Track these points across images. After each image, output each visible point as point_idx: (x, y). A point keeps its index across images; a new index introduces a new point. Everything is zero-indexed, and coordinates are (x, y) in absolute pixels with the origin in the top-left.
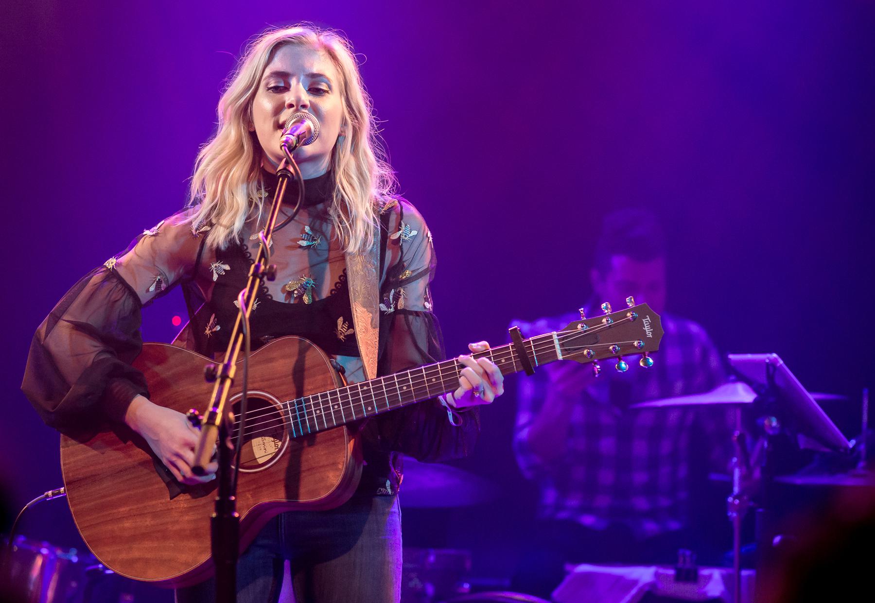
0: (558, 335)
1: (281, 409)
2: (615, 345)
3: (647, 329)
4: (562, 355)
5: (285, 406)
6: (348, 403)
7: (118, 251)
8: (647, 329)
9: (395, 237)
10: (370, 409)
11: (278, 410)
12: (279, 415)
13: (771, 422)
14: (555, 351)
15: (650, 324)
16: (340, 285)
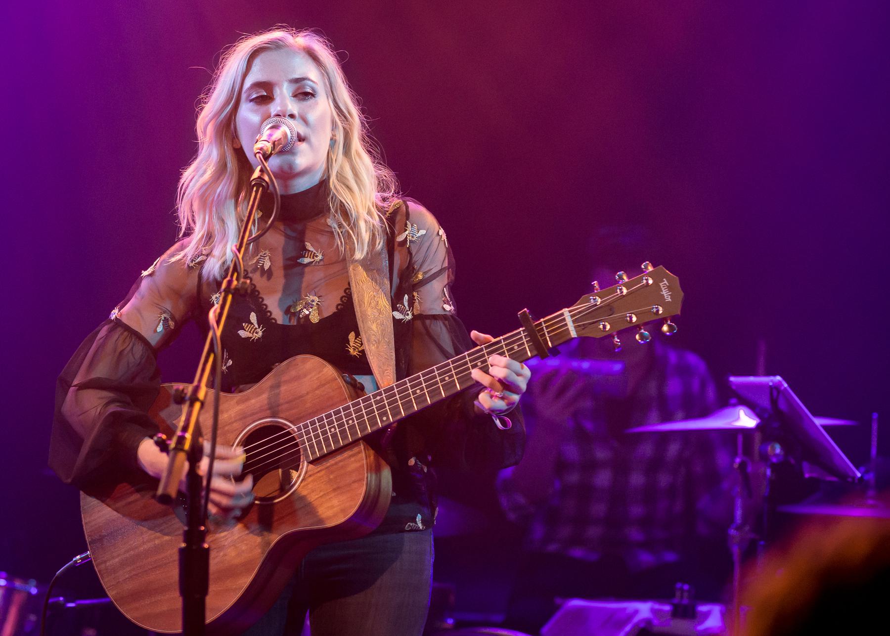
0: (570, 312)
2: (630, 313)
3: (665, 292)
5: (299, 429)
6: (362, 416)
7: (121, 298)
8: (665, 292)
10: (385, 419)
11: (292, 434)
12: (293, 439)
14: (568, 329)
15: (668, 287)
16: (346, 299)
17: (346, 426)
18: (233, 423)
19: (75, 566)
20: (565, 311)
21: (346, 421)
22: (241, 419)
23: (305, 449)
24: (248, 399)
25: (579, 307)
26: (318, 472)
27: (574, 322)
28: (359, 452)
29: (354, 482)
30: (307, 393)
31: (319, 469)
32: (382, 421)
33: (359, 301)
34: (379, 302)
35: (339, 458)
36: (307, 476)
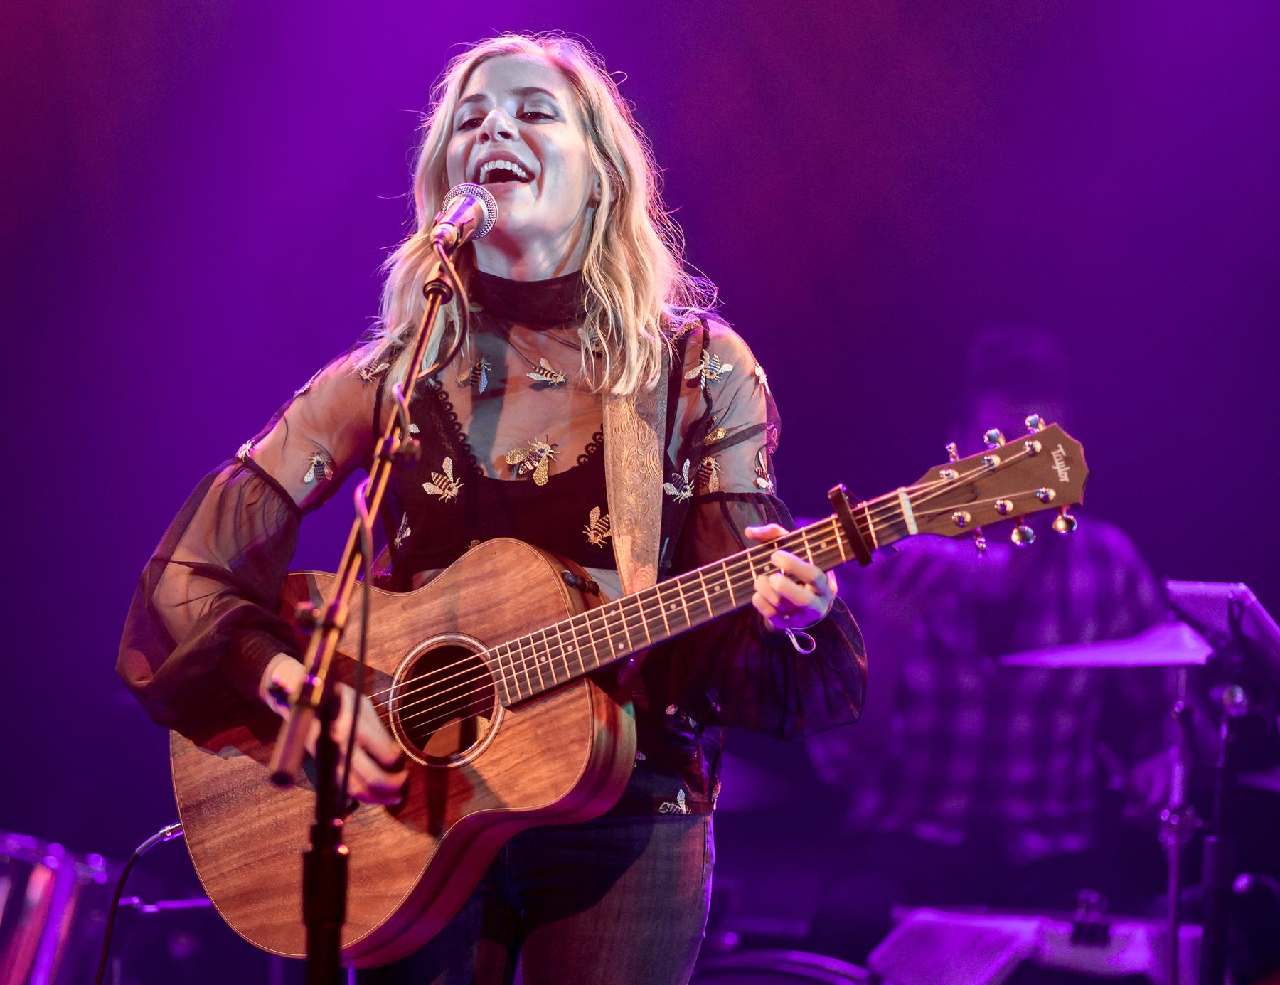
1: (488, 660)
4: (918, 526)
5: (494, 656)
9: (690, 375)
10: (621, 646)
11: (483, 662)
12: (485, 669)
13: (1232, 695)
14: (904, 521)
17: (564, 655)
18: (394, 639)
19: (161, 844)
20: (901, 491)
21: (564, 647)
22: (407, 633)
23: (501, 688)
24: (418, 603)
25: (926, 486)
26: (520, 723)
27: (915, 509)
28: (582, 696)
29: (572, 742)
30: (508, 599)
31: (521, 719)
32: (617, 650)
33: (613, 456)
34: (645, 463)
35: (551, 703)
36: (502, 729)
